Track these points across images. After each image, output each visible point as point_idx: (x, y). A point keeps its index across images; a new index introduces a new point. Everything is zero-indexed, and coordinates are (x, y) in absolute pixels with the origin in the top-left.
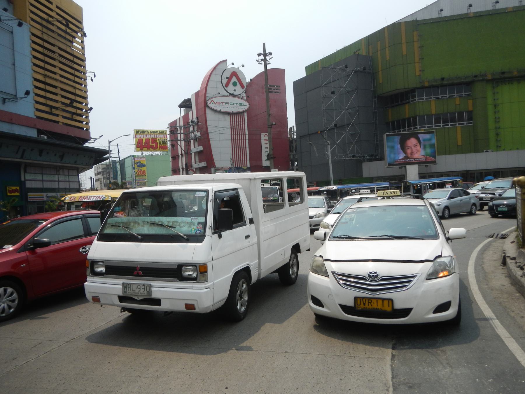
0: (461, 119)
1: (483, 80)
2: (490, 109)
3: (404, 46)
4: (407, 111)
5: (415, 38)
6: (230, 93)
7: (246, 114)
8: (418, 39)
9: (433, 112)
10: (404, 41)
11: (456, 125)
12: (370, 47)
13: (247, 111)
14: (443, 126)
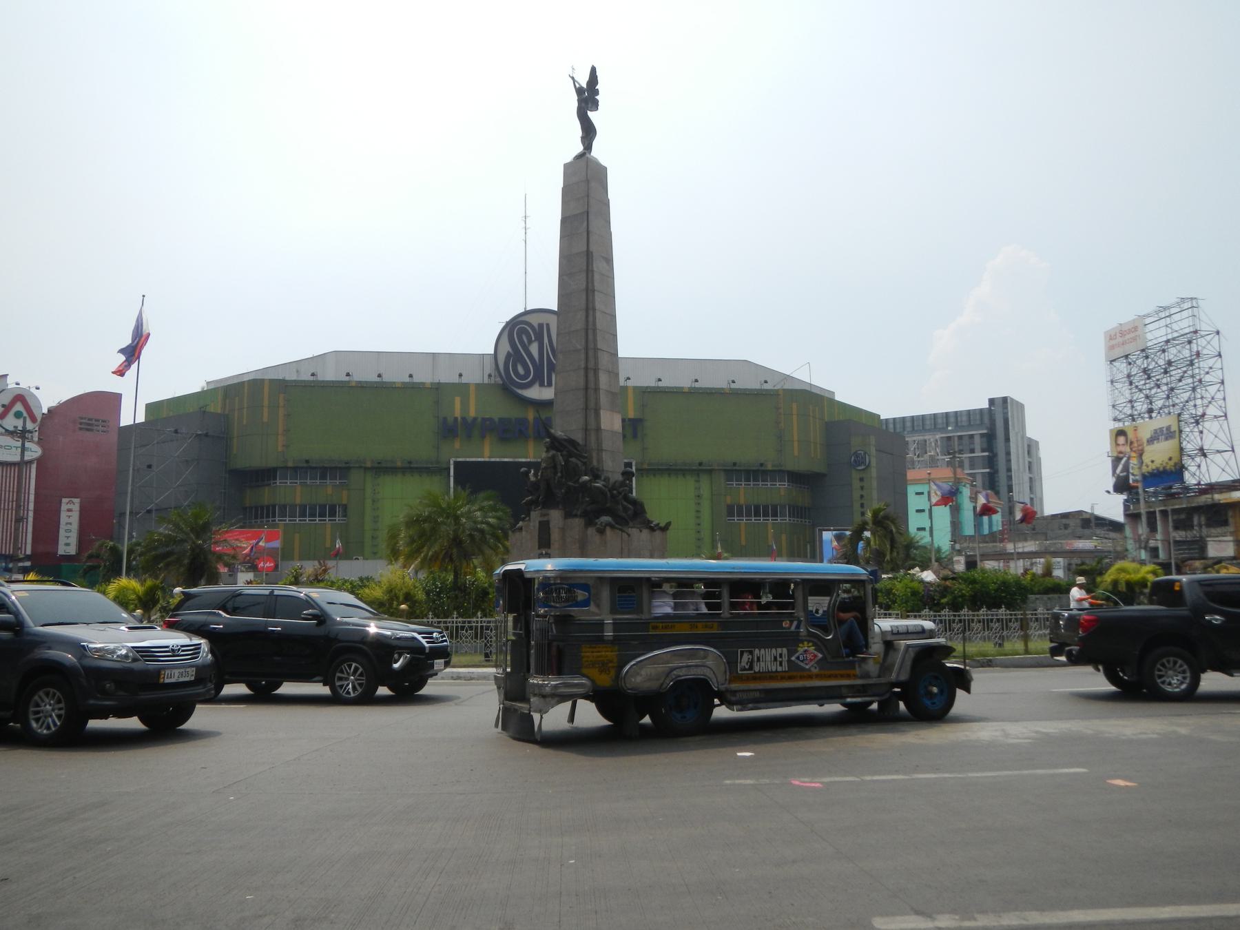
0: (333, 514)
1: (361, 467)
2: (368, 502)
3: (266, 410)
4: (266, 496)
5: (282, 404)
6: (6, 430)
7: (34, 466)
8: (285, 405)
9: (298, 501)
10: (266, 402)
11: (325, 520)
12: (228, 401)
13: (39, 461)
14: (309, 520)
